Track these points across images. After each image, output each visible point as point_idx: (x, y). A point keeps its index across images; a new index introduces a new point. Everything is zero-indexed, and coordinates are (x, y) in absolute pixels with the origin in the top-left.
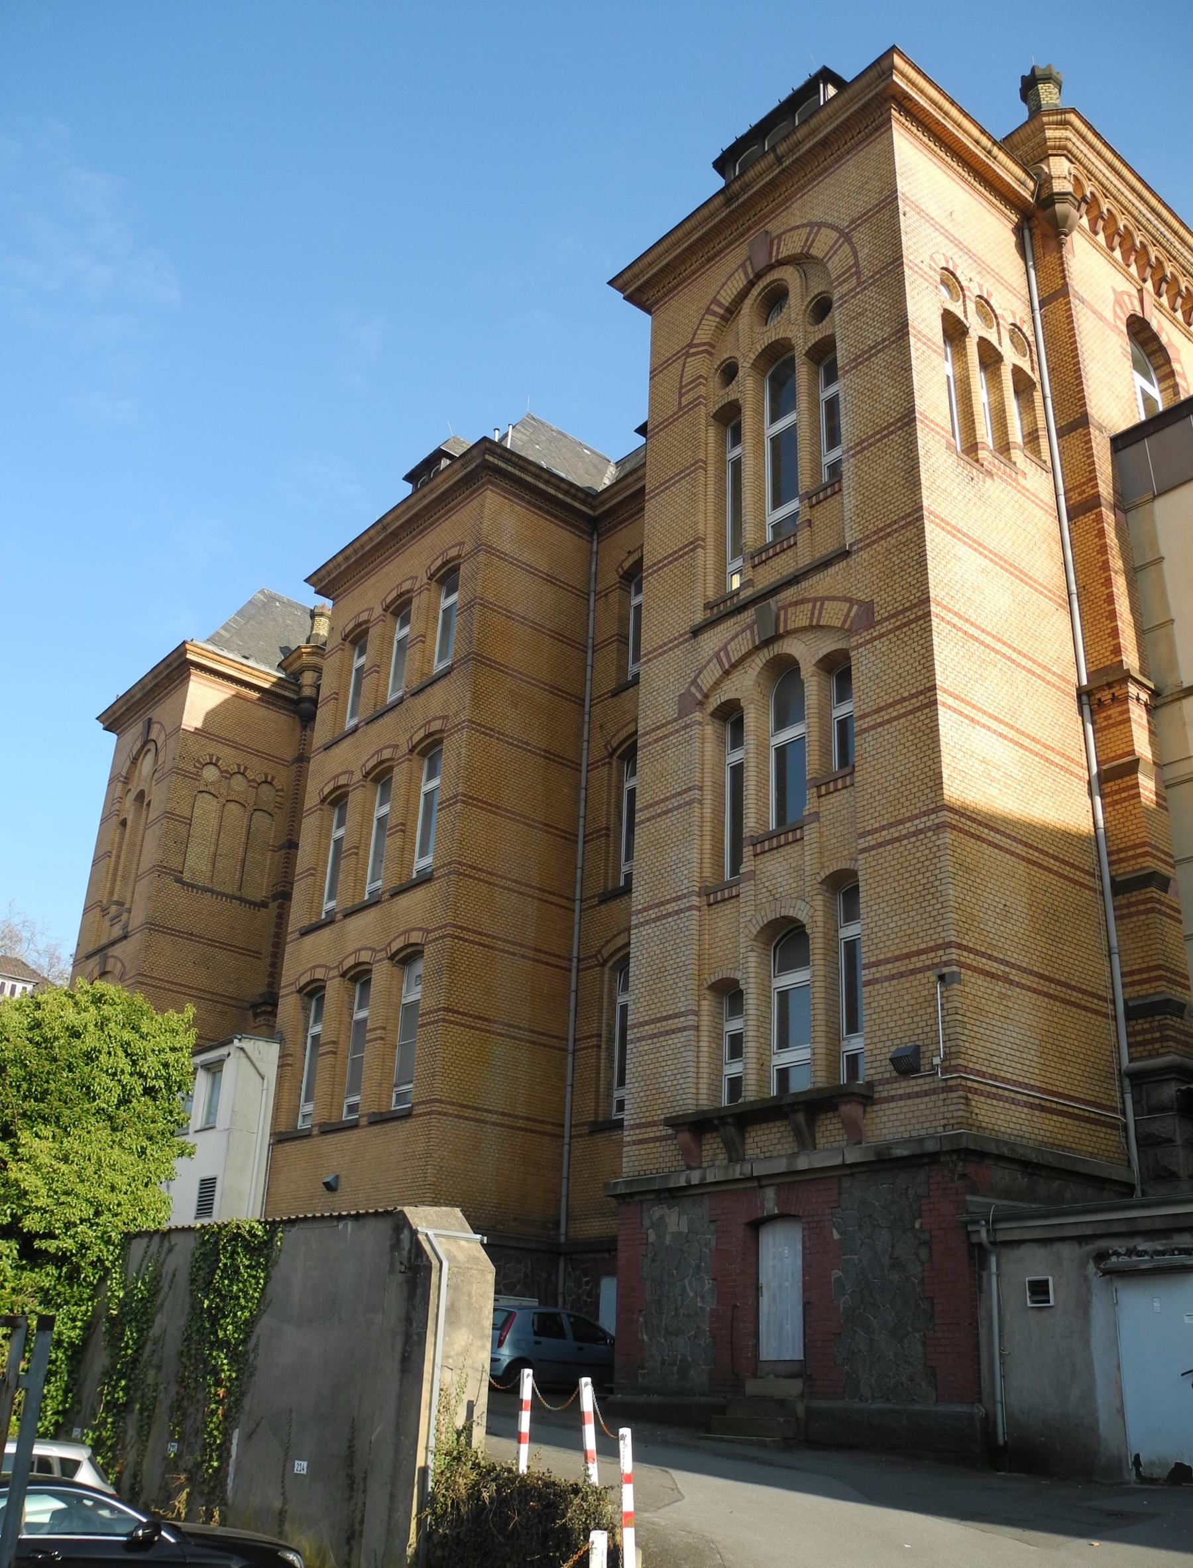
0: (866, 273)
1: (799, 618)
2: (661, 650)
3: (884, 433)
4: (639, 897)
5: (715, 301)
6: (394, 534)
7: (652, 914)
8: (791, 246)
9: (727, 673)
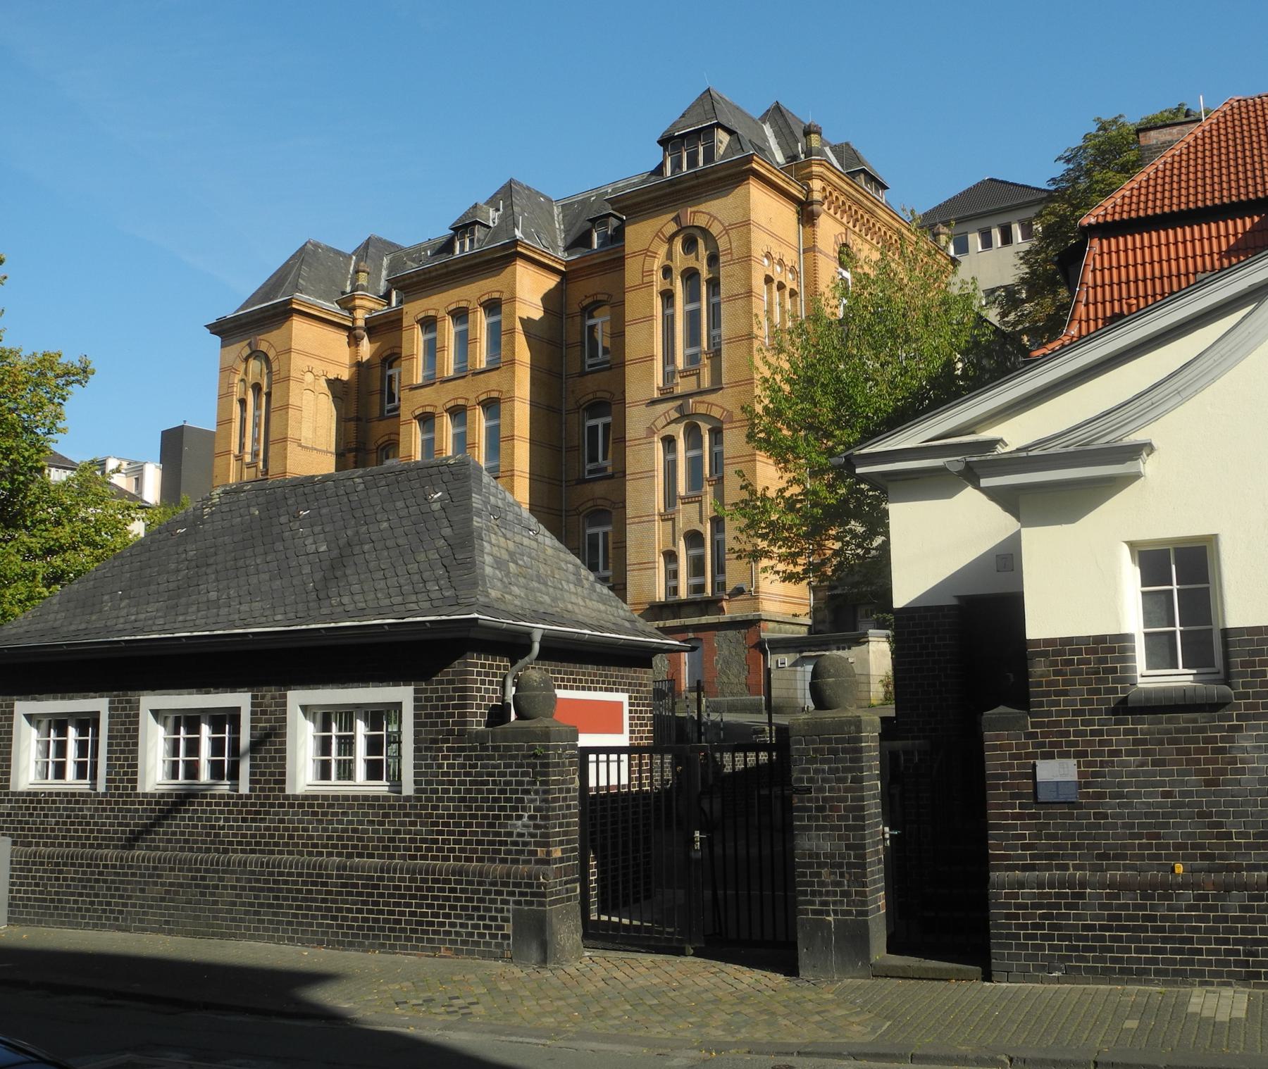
0: (735, 257)
1: (702, 409)
2: (635, 403)
3: (739, 338)
4: (630, 512)
5: (660, 231)
6: (454, 272)
7: (636, 520)
8: (701, 221)
9: (668, 424)
